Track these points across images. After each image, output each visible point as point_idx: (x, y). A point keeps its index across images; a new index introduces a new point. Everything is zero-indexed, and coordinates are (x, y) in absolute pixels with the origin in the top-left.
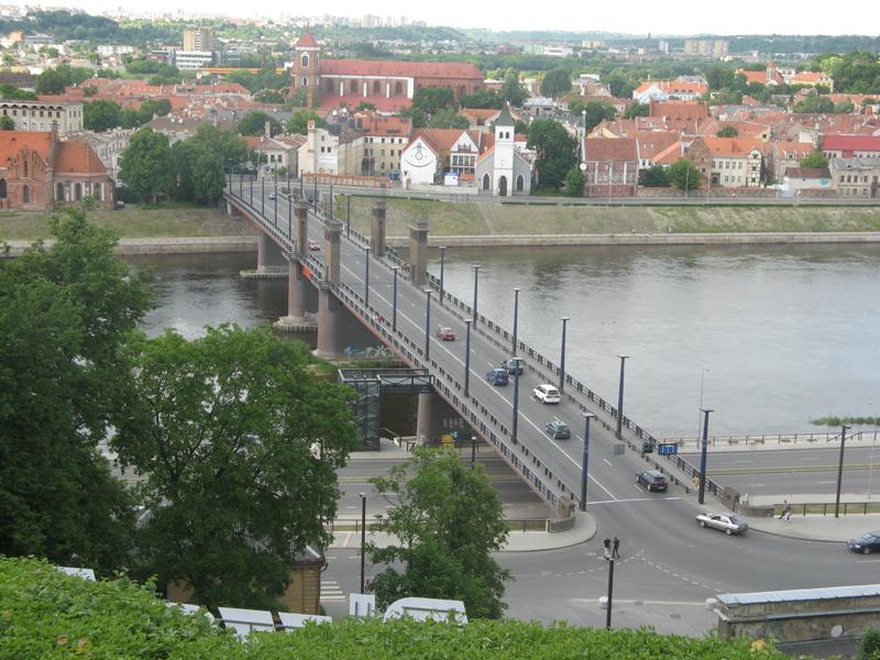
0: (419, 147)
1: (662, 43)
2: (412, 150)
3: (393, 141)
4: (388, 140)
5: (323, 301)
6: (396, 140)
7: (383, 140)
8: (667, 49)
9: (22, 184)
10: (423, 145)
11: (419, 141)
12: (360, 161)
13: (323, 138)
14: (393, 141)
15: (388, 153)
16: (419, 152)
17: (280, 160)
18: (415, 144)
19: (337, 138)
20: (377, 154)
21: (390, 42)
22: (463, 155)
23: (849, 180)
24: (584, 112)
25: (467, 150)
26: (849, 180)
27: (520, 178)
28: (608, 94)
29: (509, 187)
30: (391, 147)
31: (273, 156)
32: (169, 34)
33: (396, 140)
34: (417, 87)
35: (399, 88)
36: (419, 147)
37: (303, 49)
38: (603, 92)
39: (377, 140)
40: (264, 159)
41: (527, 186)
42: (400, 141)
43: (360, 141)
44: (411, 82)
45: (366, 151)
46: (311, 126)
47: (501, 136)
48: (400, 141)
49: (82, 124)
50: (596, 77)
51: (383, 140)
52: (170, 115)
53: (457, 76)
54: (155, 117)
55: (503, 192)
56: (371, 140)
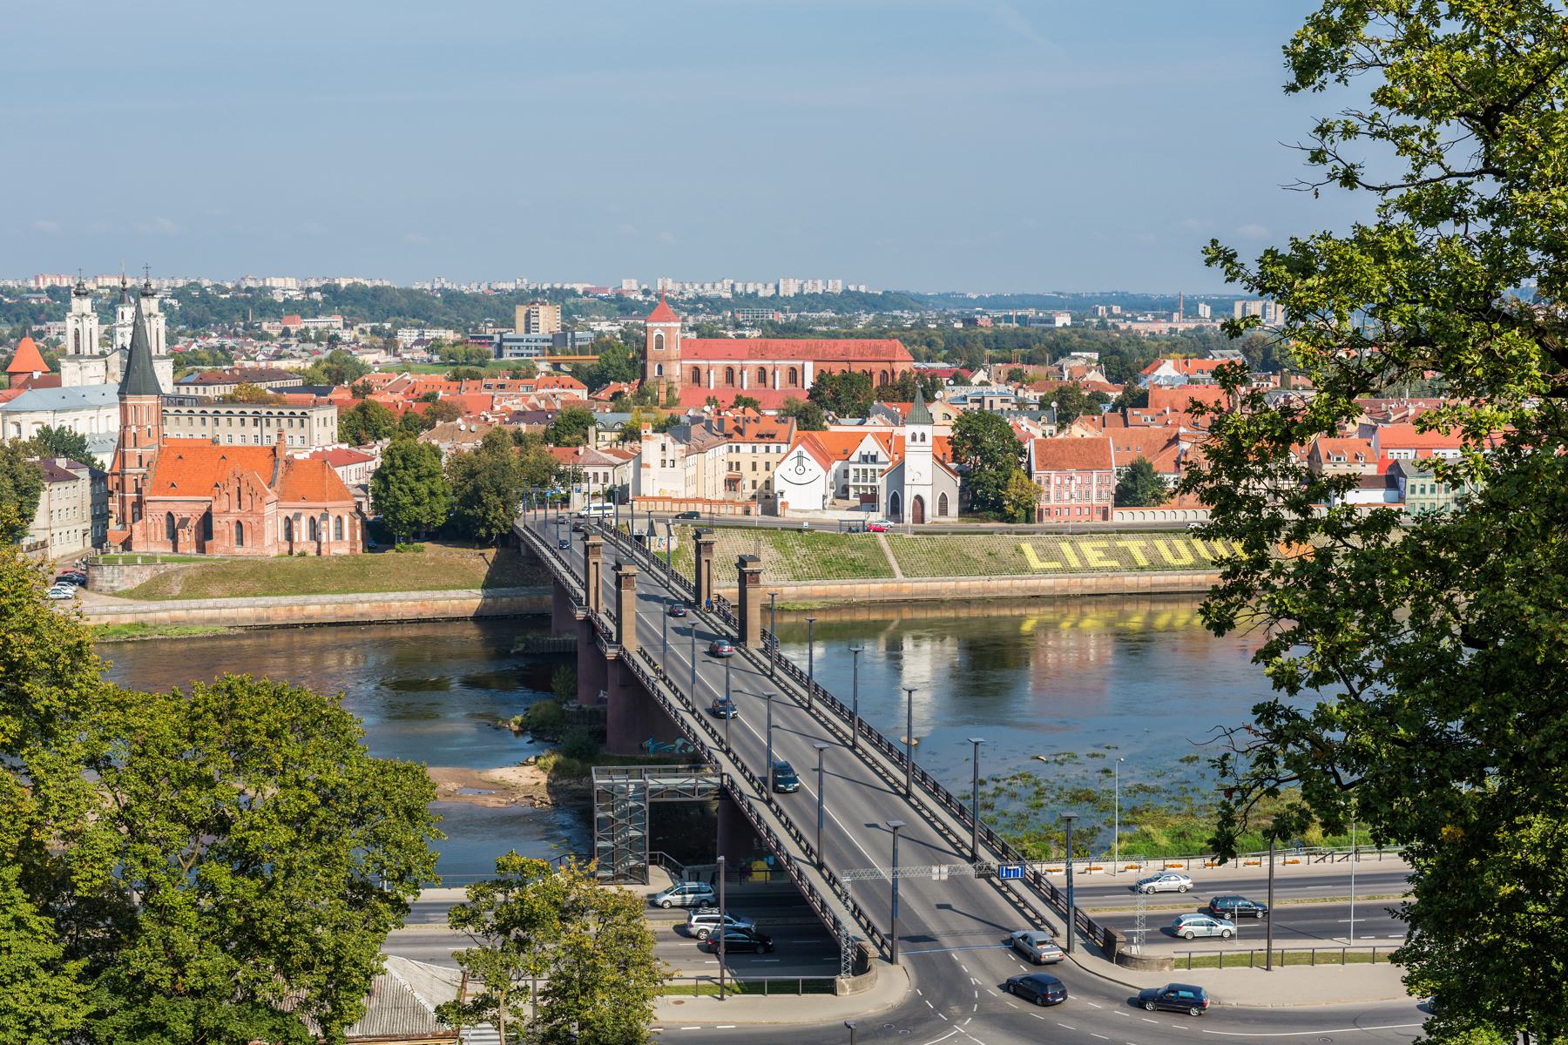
0: (800, 456)
1: (1201, 306)
2: (790, 463)
3: (768, 450)
4: (761, 448)
5: (614, 675)
6: (773, 447)
7: (754, 450)
8: (1208, 315)
9: (232, 519)
10: (806, 454)
11: (800, 448)
12: (721, 481)
13: (664, 448)
14: (768, 450)
15: (761, 467)
16: (800, 463)
17: (606, 479)
18: (794, 454)
19: (683, 447)
20: (746, 469)
21: (815, 315)
22: (869, 467)
23: (1423, 491)
24: (1054, 404)
25: (874, 459)
26: (1423, 491)
27: (944, 497)
28: (1101, 379)
29: (928, 511)
30: (767, 458)
31: (596, 474)
32: (502, 307)
33: (773, 447)
34: (821, 378)
35: (793, 375)
36: (800, 456)
37: (656, 325)
38: (1096, 377)
39: (746, 448)
40: (578, 478)
41: (953, 508)
42: (778, 451)
43: (723, 449)
44: (809, 366)
45: (731, 464)
46: (647, 430)
47: (914, 438)
48: (778, 451)
49: (336, 436)
50: (1096, 356)
51: (754, 450)
52: (459, 421)
53: (873, 358)
54: (439, 423)
55: (919, 517)
56: (738, 448)
